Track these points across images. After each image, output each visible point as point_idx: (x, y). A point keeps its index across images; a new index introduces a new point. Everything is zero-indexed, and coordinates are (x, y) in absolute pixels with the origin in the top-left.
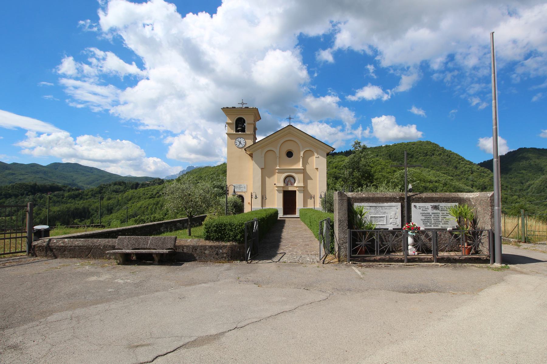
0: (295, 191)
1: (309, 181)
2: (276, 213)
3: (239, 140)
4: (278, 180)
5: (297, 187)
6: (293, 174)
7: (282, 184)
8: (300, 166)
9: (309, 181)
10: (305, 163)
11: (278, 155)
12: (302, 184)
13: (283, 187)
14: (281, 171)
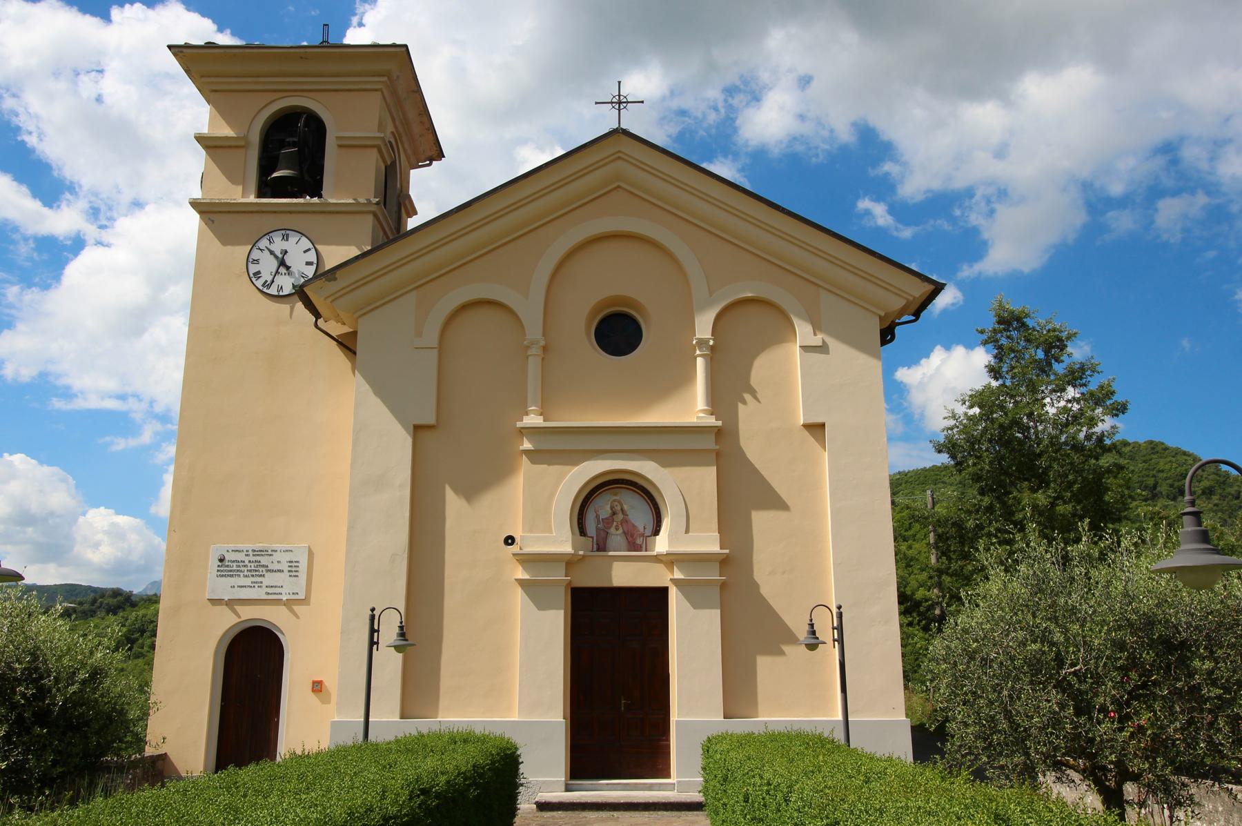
0: (664, 591)
1: (761, 520)
2: (499, 772)
3: (278, 245)
4: (535, 510)
5: (671, 560)
6: (647, 469)
7: (562, 541)
8: (692, 407)
9: (761, 520)
10: (728, 389)
11: (534, 330)
12: (708, 543)
13: (570, 562)
14: (557, 447)
